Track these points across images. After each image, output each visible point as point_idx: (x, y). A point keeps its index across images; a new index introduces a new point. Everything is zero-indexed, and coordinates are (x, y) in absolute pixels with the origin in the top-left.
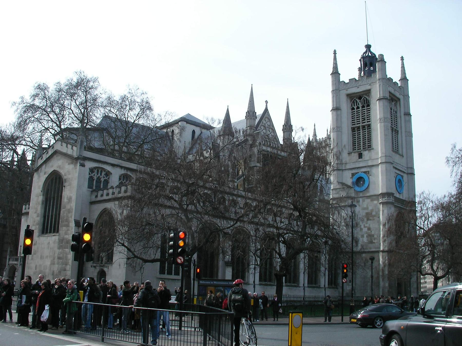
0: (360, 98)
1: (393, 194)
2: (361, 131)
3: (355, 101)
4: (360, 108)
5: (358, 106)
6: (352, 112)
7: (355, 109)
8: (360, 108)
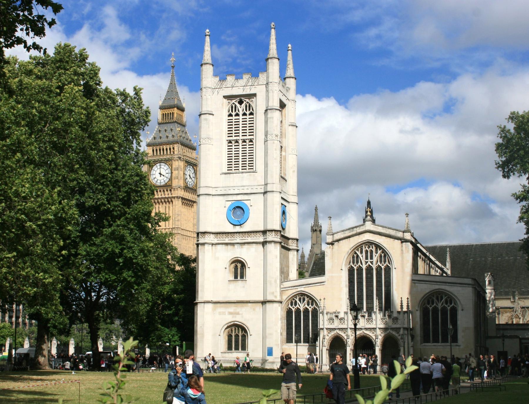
0: (241, 102)
1: (280, 231)
2: (241, 147)
3: (234, 105)
4: (241, 117)
5: (237, 113)
6: (228, 120)
7: (234, 116)
8: (241, 117)
